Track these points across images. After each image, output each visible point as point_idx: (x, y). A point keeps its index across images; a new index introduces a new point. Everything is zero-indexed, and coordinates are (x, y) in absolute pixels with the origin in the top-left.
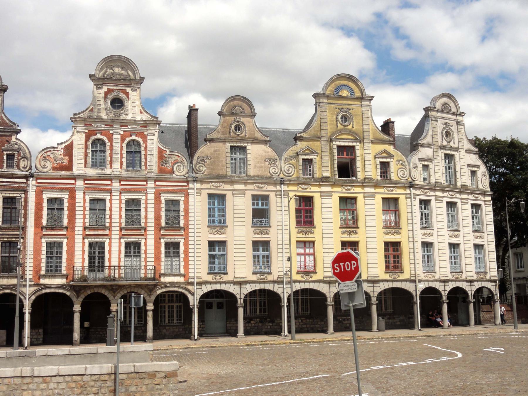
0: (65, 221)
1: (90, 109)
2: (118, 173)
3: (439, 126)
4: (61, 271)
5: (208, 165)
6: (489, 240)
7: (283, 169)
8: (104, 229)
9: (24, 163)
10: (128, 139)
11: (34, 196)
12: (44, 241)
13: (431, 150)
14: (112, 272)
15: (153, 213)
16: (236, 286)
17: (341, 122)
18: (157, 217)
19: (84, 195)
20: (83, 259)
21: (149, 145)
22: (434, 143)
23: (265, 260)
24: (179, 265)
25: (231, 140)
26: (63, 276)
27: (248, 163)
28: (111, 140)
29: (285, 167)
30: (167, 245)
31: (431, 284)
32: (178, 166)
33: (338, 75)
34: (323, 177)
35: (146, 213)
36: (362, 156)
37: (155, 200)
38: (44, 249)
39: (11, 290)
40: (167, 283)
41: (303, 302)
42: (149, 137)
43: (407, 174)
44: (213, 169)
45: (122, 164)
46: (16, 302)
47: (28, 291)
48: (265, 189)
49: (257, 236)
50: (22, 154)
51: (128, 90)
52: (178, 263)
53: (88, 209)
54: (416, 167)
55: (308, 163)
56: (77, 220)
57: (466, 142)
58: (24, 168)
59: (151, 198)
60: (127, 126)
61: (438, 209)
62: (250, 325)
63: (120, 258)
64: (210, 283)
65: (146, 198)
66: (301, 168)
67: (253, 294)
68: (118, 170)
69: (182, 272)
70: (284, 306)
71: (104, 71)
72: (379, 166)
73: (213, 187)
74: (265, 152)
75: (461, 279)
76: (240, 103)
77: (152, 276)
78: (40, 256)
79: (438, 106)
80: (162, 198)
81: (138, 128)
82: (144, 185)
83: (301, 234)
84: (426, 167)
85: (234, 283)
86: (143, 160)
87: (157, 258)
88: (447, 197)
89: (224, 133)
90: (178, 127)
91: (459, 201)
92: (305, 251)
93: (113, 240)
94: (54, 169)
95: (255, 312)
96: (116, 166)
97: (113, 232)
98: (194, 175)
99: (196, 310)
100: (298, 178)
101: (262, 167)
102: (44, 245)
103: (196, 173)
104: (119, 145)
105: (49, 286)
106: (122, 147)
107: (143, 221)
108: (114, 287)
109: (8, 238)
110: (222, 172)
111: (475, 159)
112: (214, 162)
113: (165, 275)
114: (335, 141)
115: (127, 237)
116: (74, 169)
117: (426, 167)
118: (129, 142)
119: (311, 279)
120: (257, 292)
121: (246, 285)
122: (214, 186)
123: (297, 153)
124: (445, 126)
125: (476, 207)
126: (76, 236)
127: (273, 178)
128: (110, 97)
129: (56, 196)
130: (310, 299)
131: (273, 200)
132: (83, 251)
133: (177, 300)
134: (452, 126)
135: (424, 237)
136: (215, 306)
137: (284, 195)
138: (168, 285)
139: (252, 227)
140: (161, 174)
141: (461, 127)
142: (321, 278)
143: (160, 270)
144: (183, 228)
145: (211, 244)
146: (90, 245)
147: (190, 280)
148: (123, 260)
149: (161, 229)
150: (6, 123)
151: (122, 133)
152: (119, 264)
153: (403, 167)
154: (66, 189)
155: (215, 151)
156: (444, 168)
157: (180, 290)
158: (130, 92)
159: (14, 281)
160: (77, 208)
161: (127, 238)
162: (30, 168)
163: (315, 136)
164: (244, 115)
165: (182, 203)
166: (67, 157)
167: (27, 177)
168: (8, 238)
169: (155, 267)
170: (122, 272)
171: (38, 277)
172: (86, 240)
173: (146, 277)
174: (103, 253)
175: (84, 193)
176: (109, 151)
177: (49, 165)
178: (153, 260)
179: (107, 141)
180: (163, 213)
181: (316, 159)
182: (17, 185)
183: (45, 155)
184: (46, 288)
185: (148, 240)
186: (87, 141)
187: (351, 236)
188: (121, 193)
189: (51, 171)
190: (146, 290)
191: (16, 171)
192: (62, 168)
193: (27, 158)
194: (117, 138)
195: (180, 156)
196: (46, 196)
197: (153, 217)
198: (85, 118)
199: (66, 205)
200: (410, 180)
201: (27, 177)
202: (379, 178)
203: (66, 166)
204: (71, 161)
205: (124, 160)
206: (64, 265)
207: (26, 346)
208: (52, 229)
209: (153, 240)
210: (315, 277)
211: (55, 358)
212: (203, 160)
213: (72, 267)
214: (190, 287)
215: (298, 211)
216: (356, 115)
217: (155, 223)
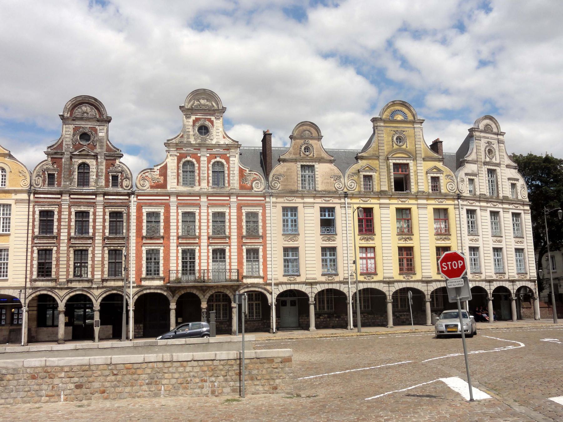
0: (162, 231)
1: (180, 136)
2: (206, 190)
3: (483, 144)
4: (158, 274)
5: (282, 182)
6: (529, 244)
7: (346, 184)
8: (194, 238)
9: (126, 182)
10: (213, 161)
11: (135, 211)
12: (144, 249)
13: (476, 166)
14: (202, 275)
15: (236, 224)
16: (307, 286)
17: (396, 143)
18: (240, 228)
19: (177, 209)
20: (177, 264)
21: (231, 165)
22: (478, 160)
23: (332, 263)
24: (259, 268)
25: (302, 160)
26: (161, 279)
27: (317, 179)
28: (199, 161)
29: (349, 183)
30: (248, 251)
32: (256, 183)
34: (381, 191)
35: (230, 224)
36: (415, 172)
37: (237, 212)
38: (144, 256)
39: (117, 290)
40: (249, 284)
41: (401, 299)
42: (231, 159)
43: (455, 187)
44: (286, 185)
45: (208, 182)
46: (123, 301)
47: (132, 291)
48: (331, 202)
49: (325, 242)
50: (124, 175)
51: (213, 118)
52: (257, 266)
53: (180, 221)
54: (463, 181)
55: (368, 178)
56: (171, 231)
57: (506, 157)
58: (127, 187)
59: (234, 211)
60: (212, 150)
61: (483, 218)
62: (319, 320)
63: (208, 263)
64: (286, 284)
65: (230, 211)
66: (362, 183)
67: (321, 293)
68: (205, 187)
69: (261, 274)
70: (349, 303)
71: (192, 103)
72: (430, 181)
73: (286, 201)
74: (331, 170)
75: (504, 279)
76: (308, 127)
77: (236, 278)
78: (141, 262)
79: (481, 127)
80: (243, 211)
82: (228, 200)
83: (363, 241)
84: (471, 181)
85: (306, 283)
86: (227, 178)
87: (240, 263)
88: (491, 207)
89: (295, 154)
90: (254, 150)
91: (501, 210)
92: (366, 255)
93: (202, 248)
94: (152, 187)
95: (324, 309)
96: (204, 184)
97: (202, 241)
98: (270, 191)
99: (274, 307)
100: (360, 192)
101: (328, 183)
102: (144, 252)
103: (272, 189)
104: (206, 166)
105: (149, 288)
106: (208, 167)
107: (227, 231)
108: (204, 288)
109: (114, 247)
110: (294, 188)
111: (514, 173)
112: (287, 179)
113: (247, 277)
114: (392, 159)
115: (214, 244)
116: (169, 187)
117: (471, 181)
118: (214, 163)
119: (372, 280)
120: (325, 291)
121: (316, 285)
122: (288, 200)
123: (358, 170)
124: (487, 144)
125: (516, 215)
126: (171, 245)
127: (338, 192)
128: (198, 125)
129: (153, 210)
130: (371, 297)
131: (338, 210)
132: (177, 257)
133: (256, 298)
134: (494, 144)
135: (471, 242)
136: (288, 304)
137: (348, 207)
138: (250, 286)
139: (321, 235)
140: (242, 190)
141: (502, 145)
142: (382, 279)
143: (242, 273)
144: (261, 236)
145: (286, 250)
146: (184, 252)
147: (268, 282)
148: (211, 264)
149: (243, 237)
150: (111, 149)
151: (208, 155)
152: (208, 268)
153: (451, 181)
155: (288, 169)
156: (487, 182)
157: (260, 290)
158: (214, 120)
159: (120, 284)
160: (171, 221)
161: (214, 246)
162: (132, 187)
163: (373, 155)
164: (312, 138)
165: (260, 214)
167: (129, 195)
168: (114, 247)
169: (238, 270)
170: (210, 274)
171: (139, 280)
172: (179, 248)
173: (230, 278)
174: (194, 258)
175: (177, 207)
176: (197, 172)
177: (147, 184)
178: (236, 264)
179: (195, 163)
180: (244, 224)
182: (121, 201)
183: (144, 175)
184: (146, 289)
185: (232, 247)
186: (178, 163)
187: (407, 242)
188: (208, 207)
189: (149, 189)
191: (120, 190)
193: (128, 179)
194: (204, 159)
195: (258, 174)
196: (145, 210)
197: (236, 227)
198: (176, 144)
199: (162, 218)
200: (457, 192)
201: (129, 195)
202: (430, 191)
203: (161, 184)
204: (165, 180)
205: (210, 178)
206: (161, 269)
207: (131, 338)
208: (151, 238)
209: (236, 247)
210: (376, 278)
211: (174, 347)
212: (277, 177)
213: (168, 271)
214: (268, 288)
215: (360, 220)
216: (409, 136)
217: (238, 233)
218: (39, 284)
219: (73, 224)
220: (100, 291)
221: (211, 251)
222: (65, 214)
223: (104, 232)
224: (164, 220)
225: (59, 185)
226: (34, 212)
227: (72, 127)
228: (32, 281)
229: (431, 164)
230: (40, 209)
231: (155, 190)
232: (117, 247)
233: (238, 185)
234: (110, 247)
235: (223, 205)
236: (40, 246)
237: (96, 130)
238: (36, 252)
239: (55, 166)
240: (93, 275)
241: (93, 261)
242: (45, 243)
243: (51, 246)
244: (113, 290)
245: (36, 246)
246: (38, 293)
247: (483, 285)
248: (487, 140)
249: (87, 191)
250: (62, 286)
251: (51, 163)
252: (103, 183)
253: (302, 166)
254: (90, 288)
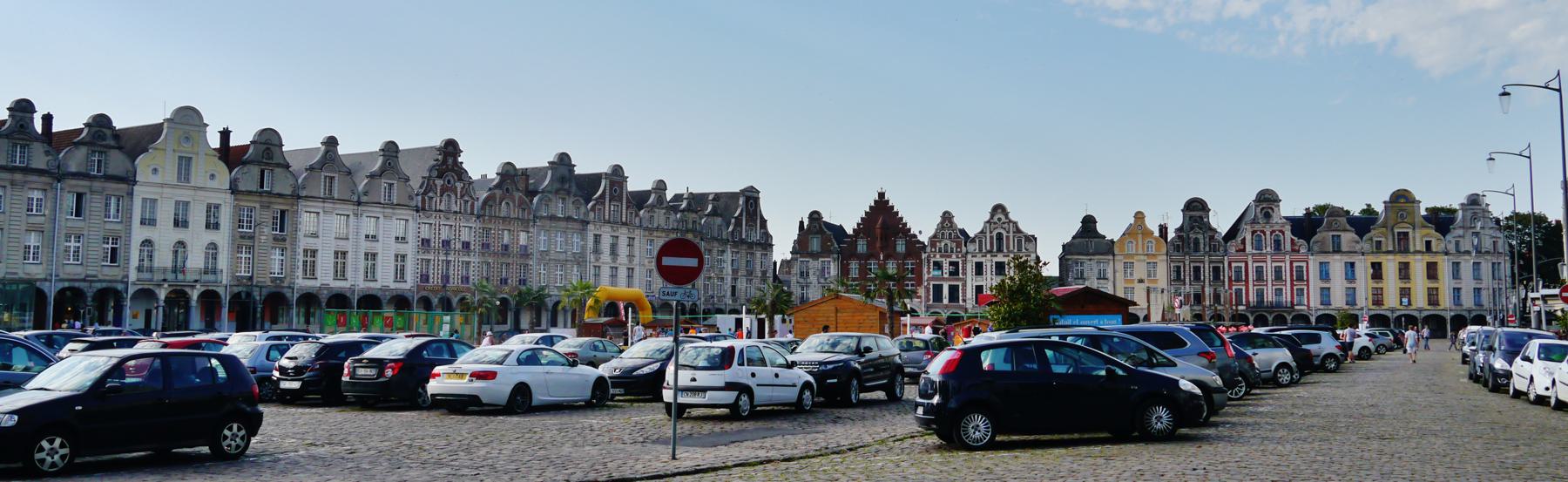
18: (1292, 275)
28: (1265, 235)
31: (1459, 313)
51: (1273, 207)
55: (1379, 243)
94: (1237, 251)
96: (1269, 249)
116: (1247, 250)
117: (1457, 244)
194: (1268, 233)
196: (1233, 265)
204: (1245, 247)
210: (1383, 307)
213: (1247, 301)
247: (1464, 313)
253: (1333, 236)
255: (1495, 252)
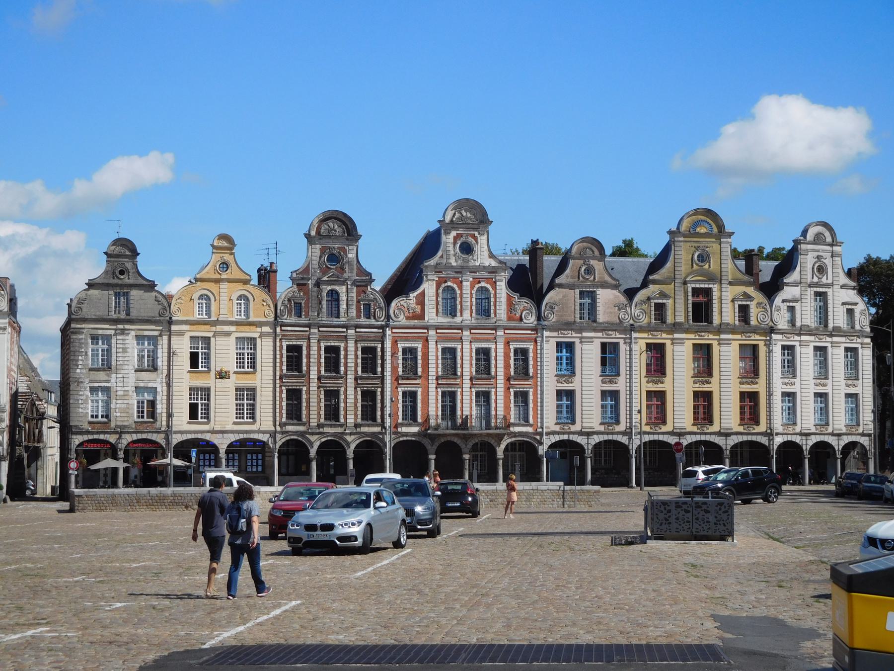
2: (468, 322)
5: (557, 311)
7: (633, 314)
10: (477, 286)
12: (400, 390)
18: (507, 366)
19: (437, 345)
20: (437, 408)
21: (498, 292)
26: (419, 425)
28: (461, 288)
31: (790, 438)
32: (527, 313)
33: (696, 210)
37: (505, 348)
44: (561, 316)
45: (471, 312)
49: (605, 385)
51: (476, 234)
54: (779, 310)
55: (660, 309)
59: (501, 346)
63: (471, 407)
67: (597, 446)
72: (737, 310)
75: (826, 432)
79: (810, 237)
80: (511, 347)
81: (485, 274)
84: (792, 309)
87: (507, 408)
89: (573, 277)
94: (408, 318)
96: (467, 314)
102: (400, 394)
105: (406, 434)
106: (471, 294)
111: (851, 295)
112: (563, 308)
113: (514, 425)
114: (690, 284)
116: (426, 318)
117: (792, 309)
123: (649, 297)
124: (816, 259)
125: (852, 352)
132: (437, 399)
133: (519, 449)
146: (443, 393)
148: (474, 408)
151: (471, 279)
154: (419, 338)
164: (594, 258)
166: (419, 306)
179: (457, 289)
180: (512, 362)
181: (669, 303)
182: (373, 334)
184: (403, 436)
188: (471, 342)
190: (497, 439)
191: (372, 321)
192: (415, 317)
194: (466, 285)
196: (401, 345)
200: (771, 324)
201: (383, 328)
202: (737, 322)
203: (418, 315)
204: (423, 310)
205: (474, 308)
206: (419, 413)
216: (714, 254)
217: (504, 372)
218: (290, 428)
219: (323, 360)
220: (353, 437)
221: (474, 394)
222: (314, 348)
223: (356, 371)
224: (422, 356)
225: (307, 315)
226: (281, 347)
227: (318, 247)
228: (282, 425)
229: (741, 289)
230: (288, 343)
231: (411, 321)
232: (371, 387)
233: (506, 316)
234: (364, 387)
235: (487, 340)
236: (288, 386)
237: (345, 251)
238: (285, 392)
239: (302, 294)
240: (346, 419)
241: (346, 403)
242: (293, 382)
243: (300, 386)
244: (368, 436)
245: (285, 386)
246: (288, 438)
248: (817, 254)
249: (337, 323)
250: (313, 431)
251: (297, 289)
252: (354, 314)
254: (343, 433)
255: (851, 332)
